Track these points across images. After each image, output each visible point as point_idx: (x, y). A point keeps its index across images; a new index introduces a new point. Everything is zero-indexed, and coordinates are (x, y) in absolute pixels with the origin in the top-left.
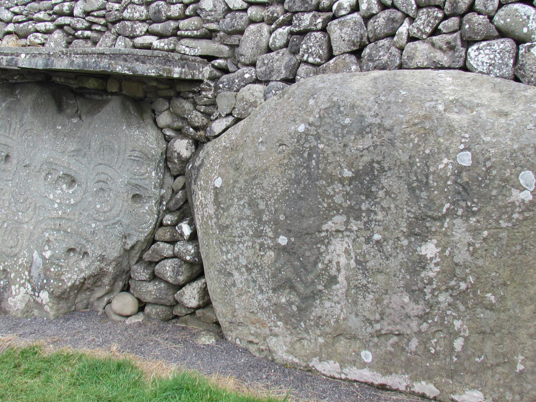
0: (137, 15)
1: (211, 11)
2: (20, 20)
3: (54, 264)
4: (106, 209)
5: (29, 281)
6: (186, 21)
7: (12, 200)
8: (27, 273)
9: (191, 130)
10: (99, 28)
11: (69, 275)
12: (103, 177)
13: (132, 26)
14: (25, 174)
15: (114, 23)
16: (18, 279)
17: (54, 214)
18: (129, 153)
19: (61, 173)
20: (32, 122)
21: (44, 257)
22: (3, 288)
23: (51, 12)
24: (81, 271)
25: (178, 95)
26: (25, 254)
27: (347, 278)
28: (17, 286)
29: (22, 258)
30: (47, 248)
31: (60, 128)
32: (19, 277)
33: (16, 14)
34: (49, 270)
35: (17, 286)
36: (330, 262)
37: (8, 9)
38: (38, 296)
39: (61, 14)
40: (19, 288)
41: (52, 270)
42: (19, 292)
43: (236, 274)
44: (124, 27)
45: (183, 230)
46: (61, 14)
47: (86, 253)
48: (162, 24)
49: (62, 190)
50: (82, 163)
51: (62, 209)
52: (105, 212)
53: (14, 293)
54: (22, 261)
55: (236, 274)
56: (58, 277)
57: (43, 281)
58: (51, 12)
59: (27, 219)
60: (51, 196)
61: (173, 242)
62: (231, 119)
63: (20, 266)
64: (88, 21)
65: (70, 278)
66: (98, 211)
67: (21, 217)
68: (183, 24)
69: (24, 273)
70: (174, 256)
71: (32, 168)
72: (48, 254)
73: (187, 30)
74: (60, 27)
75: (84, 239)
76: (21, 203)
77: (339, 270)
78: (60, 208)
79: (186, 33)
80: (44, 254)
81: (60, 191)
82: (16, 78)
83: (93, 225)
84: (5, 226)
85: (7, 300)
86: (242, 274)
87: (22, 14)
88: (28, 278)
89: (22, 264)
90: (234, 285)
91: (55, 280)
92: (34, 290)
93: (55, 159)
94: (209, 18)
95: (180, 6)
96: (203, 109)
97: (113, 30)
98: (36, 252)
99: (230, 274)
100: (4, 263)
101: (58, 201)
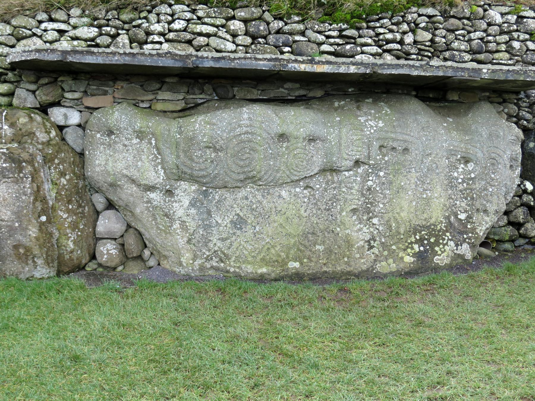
0: (463, 47)
1: (519, 49)
2: (341, 43)
3: (469, 222)
4: (498, 177)
6: (501, 55)
7: (418, 183)
8: (448, 234)
9: (525, 122)
10: (430, 54)
11: (480, 228)
12: (493, 155)
13: (459, 55)
14: (429, 161)
15: (441, 52)
16: (441, 241)
17: (461, 187)
18: (510, 138)
19: (459, 156)
20: (428, 121)
21: (460, 219)
23: (377, 39)
24: (487, 223)
25: (505, 101)
26: (441, 221)
29: (440, 225)
30: (459, 212)
31: (445, 125)
33: (328, 37)
34: (467, 227)
35: (441, 246)
37: (320, 32)
39: (388, 42)
40: (444, 248)
41: (469, 227)
42: (445, 250)
44: (454, 55)
45: (527, 187)
46: (388, 42)
47: (485, 211)
48: (484, 54)
49: (463, 168)
50: (476, 147)
51: (465, 182)
52: (497, 179)
53: (439, 252)
56: (473, 231)
57: (463, 237)
58: (377, 39)
59: (436, 195)
60: (456, 174)
61: (520, 196)
63: (439, 231)
65: (481, 230)
66: (493, 180)
67: (429, 194)
68: (496, 55)
69: (446, 236)
70: (522, 205)
71: (433, 156)
72: (462, 216)
73: (501, 60)
74: (389, 51)
75: (485, 201)
76: (428, 184)
78: (463, 182)
79: (503, 62)
80: (459, 217)
82: (350, 90)
83: (491, 190)
84: (414, 204)
85: (433, 260)
88: (450, 237)
91: (472, 233)
92: (457, 245)
93: (454, 146)
94: (518, 53)
95: (495, 44)
96: (527, 110)
97: (441, 57)
98: (452, 217)
100: (420, 233)
101: (462, 177)
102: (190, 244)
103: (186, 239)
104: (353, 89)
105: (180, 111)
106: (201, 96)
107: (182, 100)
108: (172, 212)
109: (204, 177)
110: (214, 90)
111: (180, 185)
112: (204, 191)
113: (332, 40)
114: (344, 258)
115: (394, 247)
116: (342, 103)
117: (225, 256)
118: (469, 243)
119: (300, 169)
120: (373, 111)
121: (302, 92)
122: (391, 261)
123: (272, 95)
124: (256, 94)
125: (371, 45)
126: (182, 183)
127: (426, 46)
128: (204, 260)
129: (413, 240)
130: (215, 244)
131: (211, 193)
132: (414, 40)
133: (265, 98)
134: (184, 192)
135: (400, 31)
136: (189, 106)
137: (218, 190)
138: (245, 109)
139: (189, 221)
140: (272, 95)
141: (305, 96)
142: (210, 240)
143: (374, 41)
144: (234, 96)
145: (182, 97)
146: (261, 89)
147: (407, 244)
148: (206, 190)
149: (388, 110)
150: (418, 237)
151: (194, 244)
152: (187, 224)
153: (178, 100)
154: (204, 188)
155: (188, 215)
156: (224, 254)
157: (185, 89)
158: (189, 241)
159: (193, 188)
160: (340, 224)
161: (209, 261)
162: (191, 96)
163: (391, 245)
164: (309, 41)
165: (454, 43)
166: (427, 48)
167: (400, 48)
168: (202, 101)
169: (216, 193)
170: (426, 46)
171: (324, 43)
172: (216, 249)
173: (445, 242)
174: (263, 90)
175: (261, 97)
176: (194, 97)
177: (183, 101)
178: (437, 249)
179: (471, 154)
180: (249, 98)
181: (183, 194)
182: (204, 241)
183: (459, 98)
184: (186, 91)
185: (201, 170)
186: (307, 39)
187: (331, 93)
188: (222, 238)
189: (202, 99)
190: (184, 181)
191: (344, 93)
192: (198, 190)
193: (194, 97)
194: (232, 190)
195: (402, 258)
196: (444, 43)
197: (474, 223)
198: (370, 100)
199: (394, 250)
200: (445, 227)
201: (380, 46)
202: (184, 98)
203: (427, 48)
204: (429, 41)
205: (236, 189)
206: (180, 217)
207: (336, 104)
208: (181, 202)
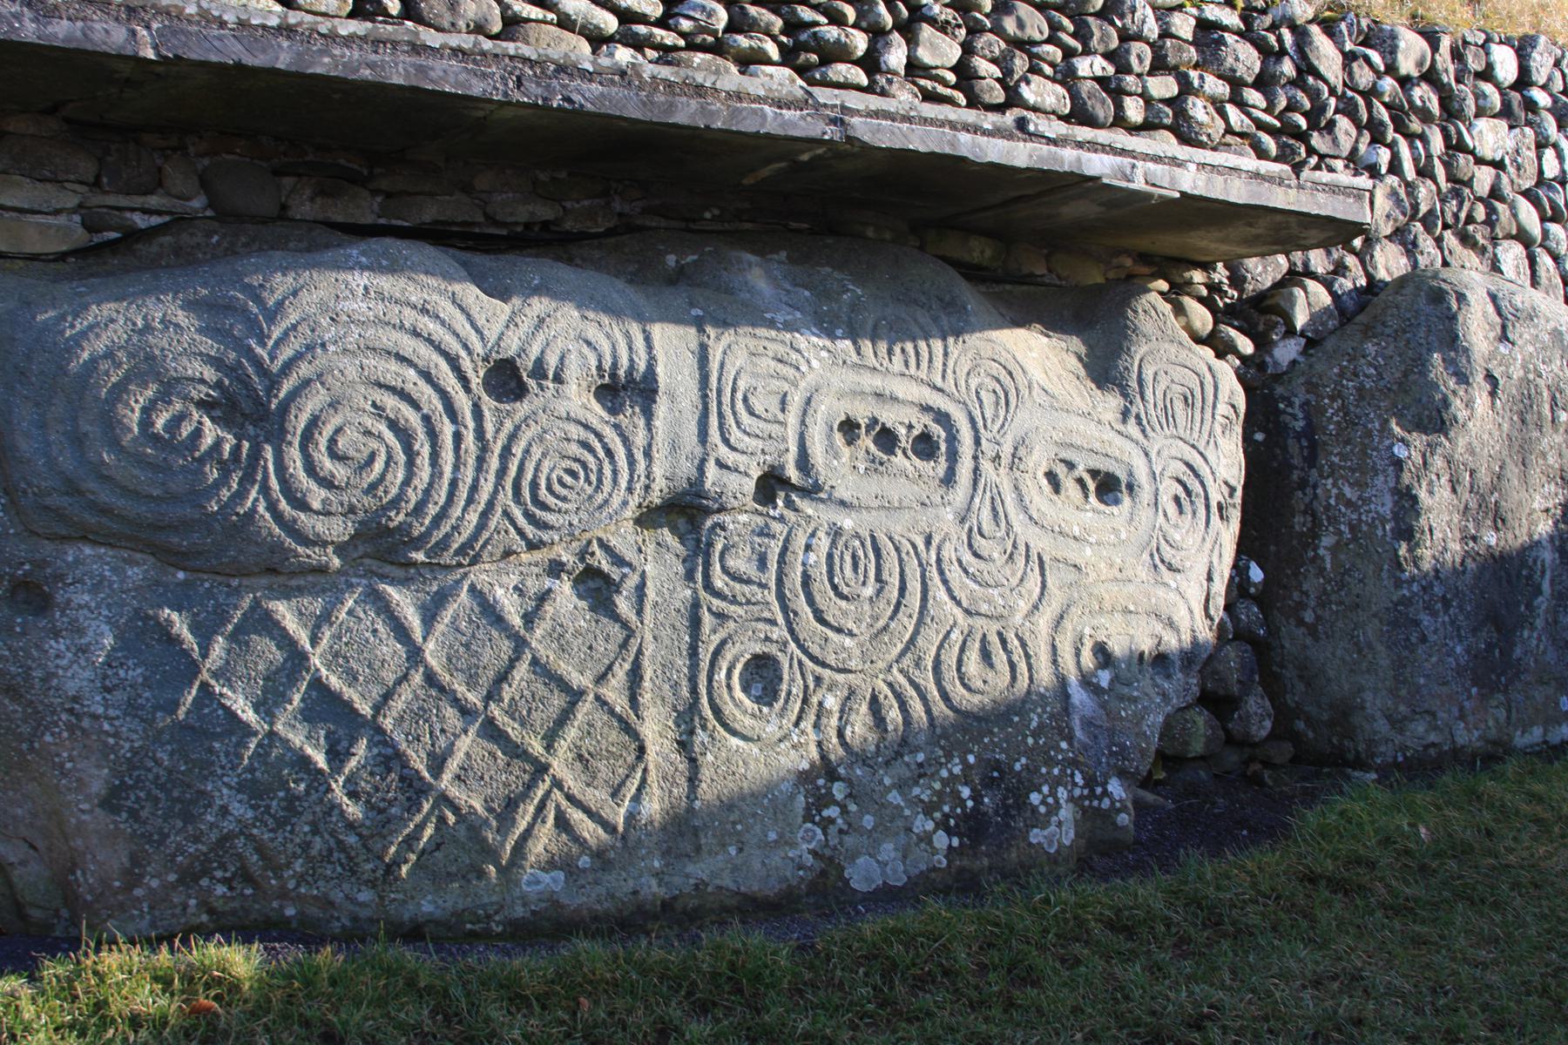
5: (1074, 763)
8: (1064, 745)
22: (997, 813)
27: (1552, 581)
28: (1045, 789)
32: (1046, 764)
35: (1045, 789)
36: (1535, 561)
38: (1105, 793)
40: (1053, 794)
42: (1057, 801)
43: (1426, 620)
54: (1040, 716)
55: (1426, 620)
60: (1076, 531)
62: (1303, 341)
64: (922, 89)
69: (1059, 750)
77: (1543, 572)
81: (1090, 514)
82: (708, 215)
86: (1434, 614)
87: (667, 27)
89: (1041, 725)
90: (1424, 639)
92: (1090, 782)
99: (1417, 623)
102: (115, 810)
103: (97, 787)
104: (716, 212)
105: (62, 257)
106: (153, 201)
107: (74, 211)
108: (37, 674)
109: (184, 526)
110: (205, 184)
111: (77, 561)
112: (178, 584)
113: (642, 29)
114: (724, 846)
115: (894, 797)
116: (691, 258)
117: (263, 857)
118: (1122, 774)
119: (564, 499)
120: (807, 293)
121: (545, 212)
122: (888, 850)
123: (429, 213)
124: (366, 210)
125: (769, 62)
126: (88, 551)
127: (945, 83)
128: (172, 877)
129: (957, 770)
130: (224, 811)
131: (210, 594)
132: (908, 57)
133: (399, 223)
134: (95, 590)
135: (864, 24)
136: (97, 239)
137: (235, 582)
138: (355, 252)
139: (111, 713)
140: (427, 218)
141: (545, 225)
142: (202, 793)
143: (780, 45)
144: (284, 207)
145: (72, 201)
146: (384, 184)
147: (937, 786)
148: (185, 584)
149: (859, 292)
150: (971, 759)
151: (134, 815)
152: (106, 727)
153: (57, 212)
154: (181, 575)
155: (108, 690)
156: (260, 849)
157: (87, 168)
158: (111, 801)
159: (135, 573)
160: (708, 712)
161: (196, 878)
162: (111, 200)
163: (888, 790)
164: (560, 25)
165: (1028, 83)
166: (948, 92)
167: (865, 81)
168: (155, 220)
169: (228, 595)
170: (945, 83)
171: (609, 40)
172: (228, 825)
173: (1056, 771)
174: (389, 195)
175: (382, 221)
176: (123, 201)
177: (77, 218)
178: (1035, 798)
179: (1116, 459)
180: (340, 219)
181: (87, 597)
182: (176, 794)
183: (1050, 271)
184: (92, 180)
185: (174, 498)
186: (551, 16)
187: (639, 222)
188: (254, 781)
189: (159, 213)
190: (95, 543)
191: (683, 225)
192: (157, 583)
193: (123, 201)
194: (294, 583)
195: (927, 838)
196: (998, 80)
197: (1135, 700)
198: (783, 254)
199: (898, 807)
200: (1052, 716)
201: (802, 71)
202: (80, 206)
203: (948, 92)
204: (952, 69)
205: (310, 578)
206: (75, 699)
207: (671, 260)
208: (81, 632)
